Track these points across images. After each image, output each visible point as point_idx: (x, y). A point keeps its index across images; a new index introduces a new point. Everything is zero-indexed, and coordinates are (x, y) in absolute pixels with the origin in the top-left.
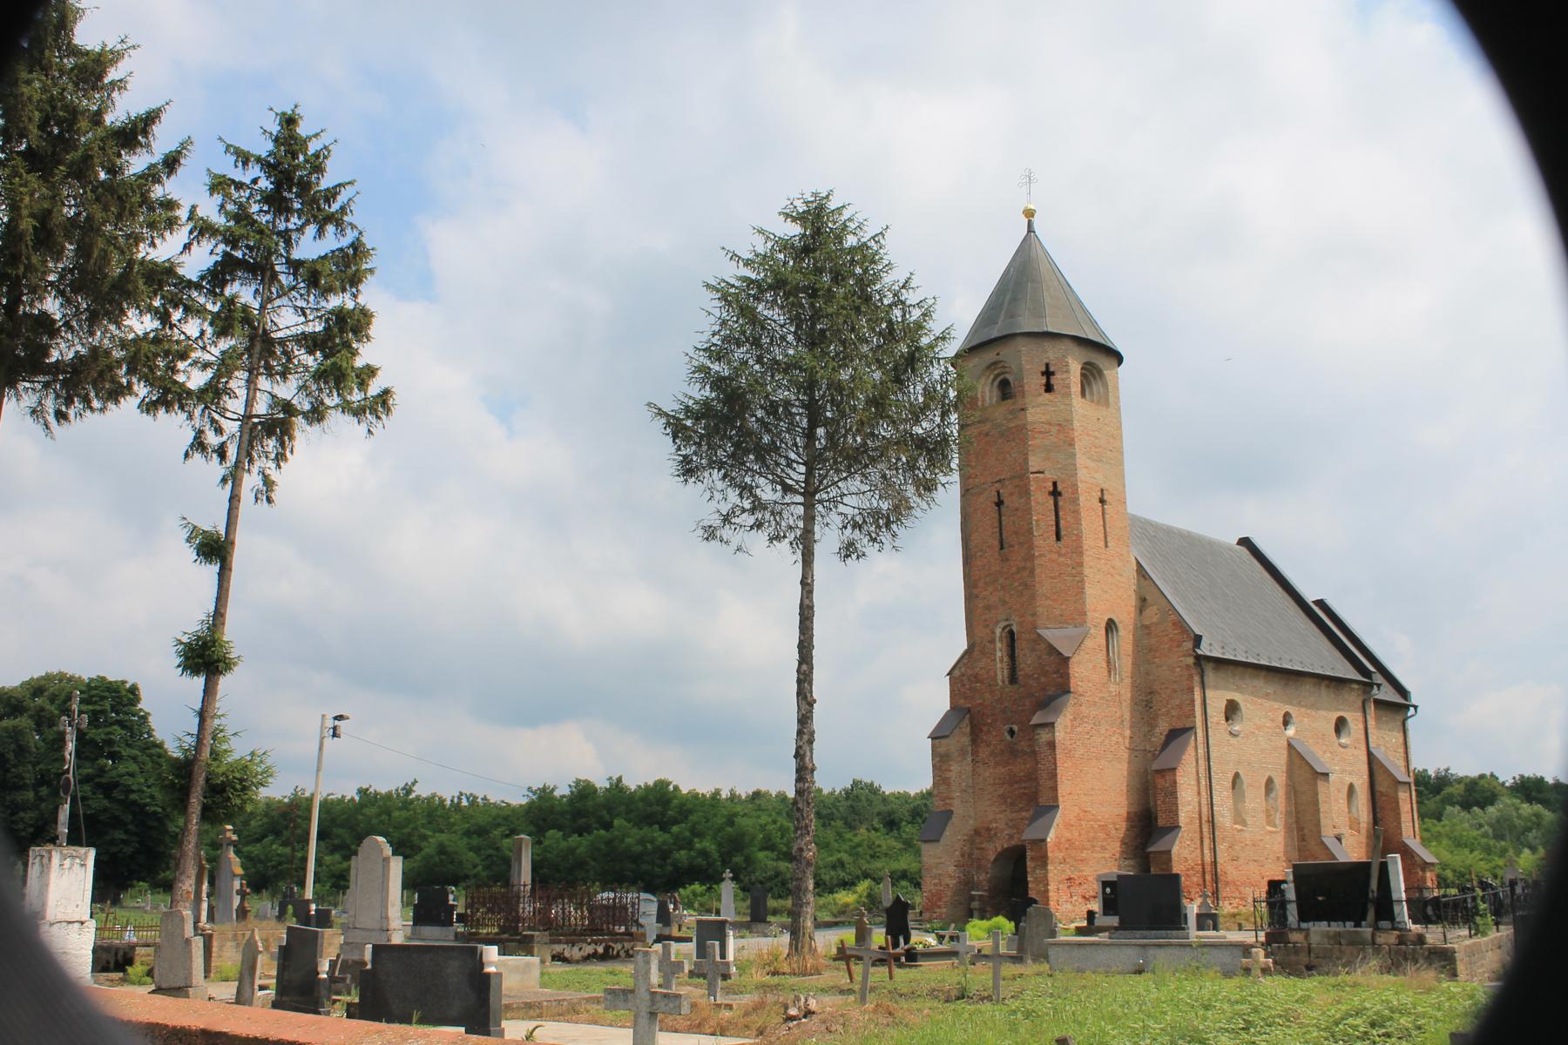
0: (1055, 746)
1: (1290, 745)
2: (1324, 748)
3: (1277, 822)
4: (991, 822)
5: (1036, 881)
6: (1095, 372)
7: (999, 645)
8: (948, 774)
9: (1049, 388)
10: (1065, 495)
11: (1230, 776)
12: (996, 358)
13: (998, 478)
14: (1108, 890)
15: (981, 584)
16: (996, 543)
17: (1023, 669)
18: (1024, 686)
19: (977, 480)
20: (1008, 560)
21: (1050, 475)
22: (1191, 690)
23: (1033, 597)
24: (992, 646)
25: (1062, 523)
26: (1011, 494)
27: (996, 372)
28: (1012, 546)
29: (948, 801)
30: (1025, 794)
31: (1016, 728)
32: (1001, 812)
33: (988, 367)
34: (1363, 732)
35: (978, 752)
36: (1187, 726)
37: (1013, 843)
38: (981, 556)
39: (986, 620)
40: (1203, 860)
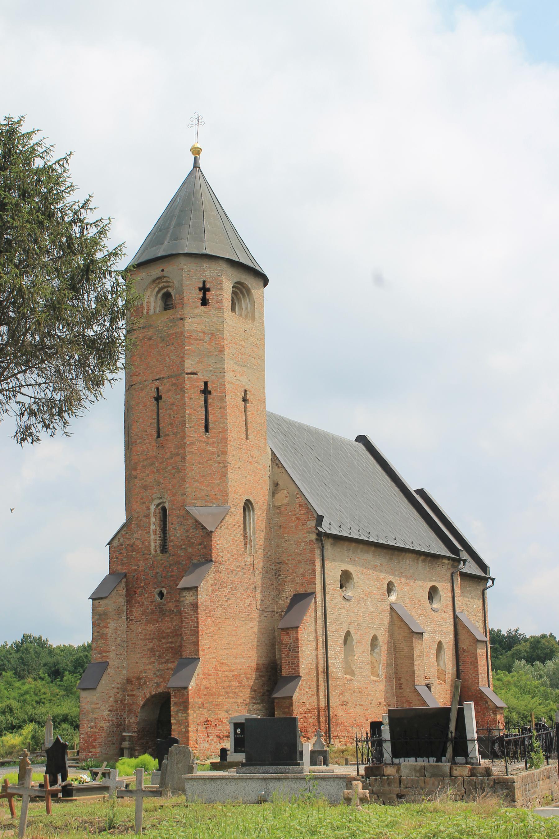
0: (197, 607)
1: (392, 608)
2: (419, 612)
3: (380, 673)
4: (141, 672)
5: (179, 723)
6: (244, 290)
7: (153, 519)
8: (105, 631)
9: (204, 302)
10: (214, 394)
11: (343, 634)
13: (157, 377)
14: (239, 731)
15: (139, 467)
16: (154, 432)
17: (172, 541)
19: (140, 378)
20: (164, 447)
21: (202, 376)
22: (313, 562)
23: (183, 479)
24: (147, 520)
25: (211, 417)
26: (169, 391)
27: (160, 286)
28: (168, 435)
29: (104, 654)
30: (171, 648)
31: (165, 591)
32: (150, 663)
33: (154, 281)
34: (451, 599)
35: (131, 611)
36: (308, 592)
37: (160, 690)
38: (140, 443)
39: (142, 498)
40: (318, 705)
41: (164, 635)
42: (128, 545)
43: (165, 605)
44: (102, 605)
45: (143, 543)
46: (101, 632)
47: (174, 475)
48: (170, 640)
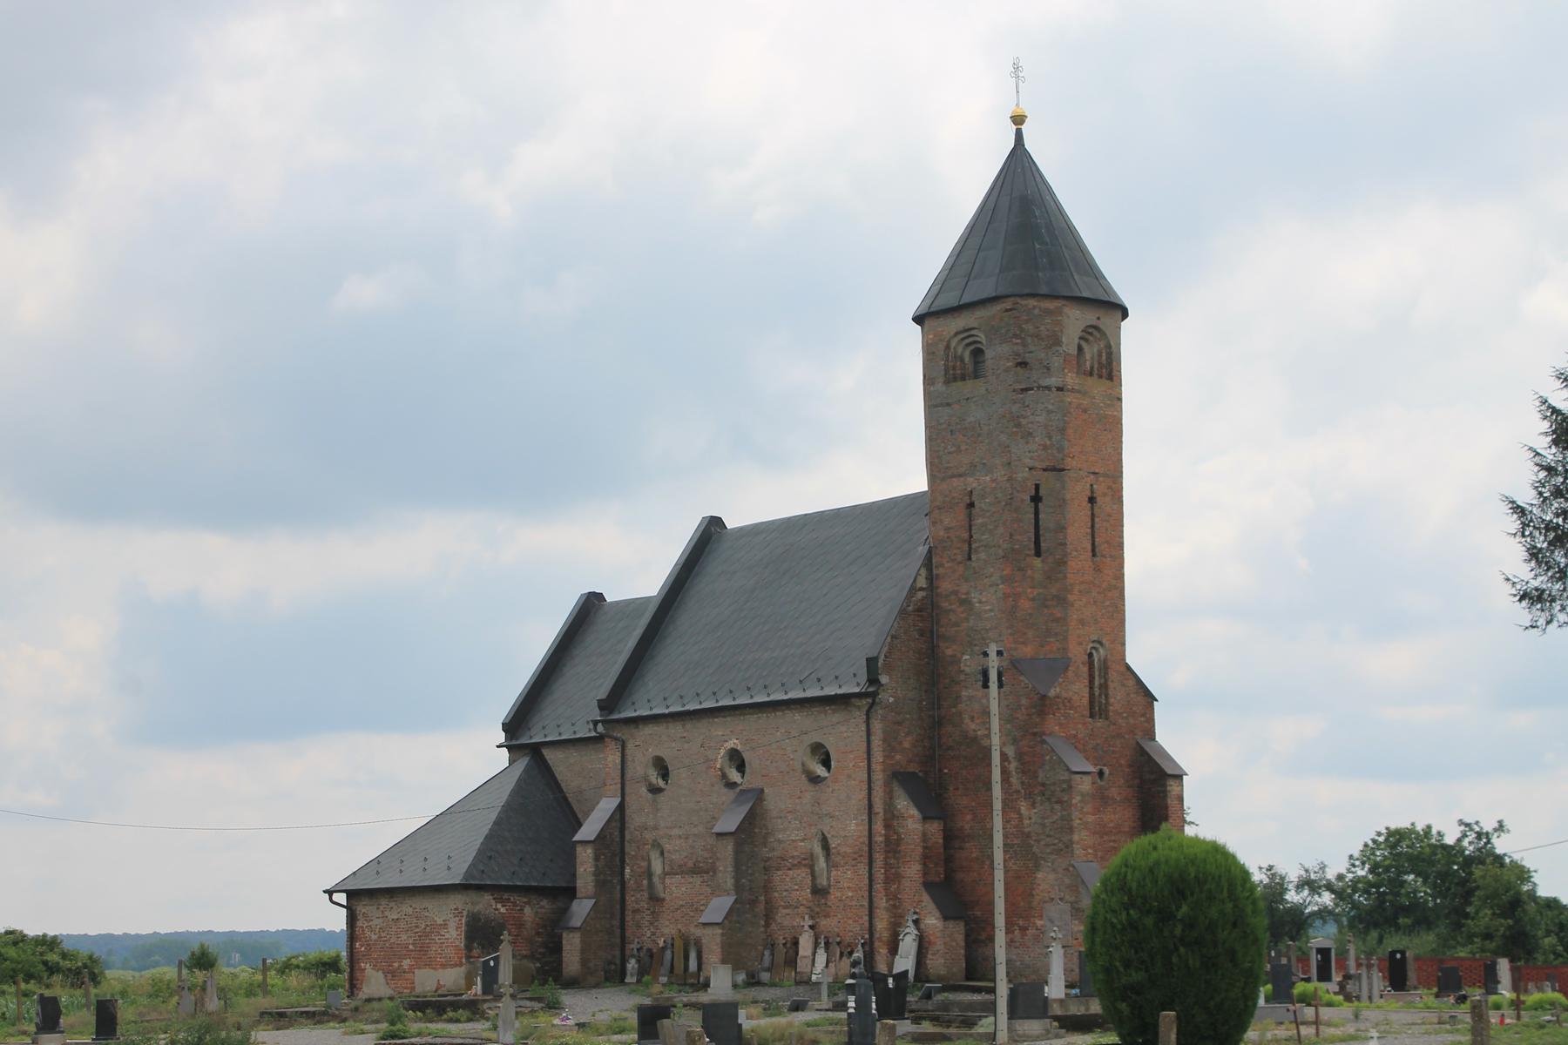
12: (1094, 322)
18: (1114, 724)
19: (1074, 462)
26: (1105, 495)
28: (1103, 556)
31: (1106, 770)
39: (1079, 637)
46: (1084, 819)
47: (1113, 615)
48: (1113, 838)
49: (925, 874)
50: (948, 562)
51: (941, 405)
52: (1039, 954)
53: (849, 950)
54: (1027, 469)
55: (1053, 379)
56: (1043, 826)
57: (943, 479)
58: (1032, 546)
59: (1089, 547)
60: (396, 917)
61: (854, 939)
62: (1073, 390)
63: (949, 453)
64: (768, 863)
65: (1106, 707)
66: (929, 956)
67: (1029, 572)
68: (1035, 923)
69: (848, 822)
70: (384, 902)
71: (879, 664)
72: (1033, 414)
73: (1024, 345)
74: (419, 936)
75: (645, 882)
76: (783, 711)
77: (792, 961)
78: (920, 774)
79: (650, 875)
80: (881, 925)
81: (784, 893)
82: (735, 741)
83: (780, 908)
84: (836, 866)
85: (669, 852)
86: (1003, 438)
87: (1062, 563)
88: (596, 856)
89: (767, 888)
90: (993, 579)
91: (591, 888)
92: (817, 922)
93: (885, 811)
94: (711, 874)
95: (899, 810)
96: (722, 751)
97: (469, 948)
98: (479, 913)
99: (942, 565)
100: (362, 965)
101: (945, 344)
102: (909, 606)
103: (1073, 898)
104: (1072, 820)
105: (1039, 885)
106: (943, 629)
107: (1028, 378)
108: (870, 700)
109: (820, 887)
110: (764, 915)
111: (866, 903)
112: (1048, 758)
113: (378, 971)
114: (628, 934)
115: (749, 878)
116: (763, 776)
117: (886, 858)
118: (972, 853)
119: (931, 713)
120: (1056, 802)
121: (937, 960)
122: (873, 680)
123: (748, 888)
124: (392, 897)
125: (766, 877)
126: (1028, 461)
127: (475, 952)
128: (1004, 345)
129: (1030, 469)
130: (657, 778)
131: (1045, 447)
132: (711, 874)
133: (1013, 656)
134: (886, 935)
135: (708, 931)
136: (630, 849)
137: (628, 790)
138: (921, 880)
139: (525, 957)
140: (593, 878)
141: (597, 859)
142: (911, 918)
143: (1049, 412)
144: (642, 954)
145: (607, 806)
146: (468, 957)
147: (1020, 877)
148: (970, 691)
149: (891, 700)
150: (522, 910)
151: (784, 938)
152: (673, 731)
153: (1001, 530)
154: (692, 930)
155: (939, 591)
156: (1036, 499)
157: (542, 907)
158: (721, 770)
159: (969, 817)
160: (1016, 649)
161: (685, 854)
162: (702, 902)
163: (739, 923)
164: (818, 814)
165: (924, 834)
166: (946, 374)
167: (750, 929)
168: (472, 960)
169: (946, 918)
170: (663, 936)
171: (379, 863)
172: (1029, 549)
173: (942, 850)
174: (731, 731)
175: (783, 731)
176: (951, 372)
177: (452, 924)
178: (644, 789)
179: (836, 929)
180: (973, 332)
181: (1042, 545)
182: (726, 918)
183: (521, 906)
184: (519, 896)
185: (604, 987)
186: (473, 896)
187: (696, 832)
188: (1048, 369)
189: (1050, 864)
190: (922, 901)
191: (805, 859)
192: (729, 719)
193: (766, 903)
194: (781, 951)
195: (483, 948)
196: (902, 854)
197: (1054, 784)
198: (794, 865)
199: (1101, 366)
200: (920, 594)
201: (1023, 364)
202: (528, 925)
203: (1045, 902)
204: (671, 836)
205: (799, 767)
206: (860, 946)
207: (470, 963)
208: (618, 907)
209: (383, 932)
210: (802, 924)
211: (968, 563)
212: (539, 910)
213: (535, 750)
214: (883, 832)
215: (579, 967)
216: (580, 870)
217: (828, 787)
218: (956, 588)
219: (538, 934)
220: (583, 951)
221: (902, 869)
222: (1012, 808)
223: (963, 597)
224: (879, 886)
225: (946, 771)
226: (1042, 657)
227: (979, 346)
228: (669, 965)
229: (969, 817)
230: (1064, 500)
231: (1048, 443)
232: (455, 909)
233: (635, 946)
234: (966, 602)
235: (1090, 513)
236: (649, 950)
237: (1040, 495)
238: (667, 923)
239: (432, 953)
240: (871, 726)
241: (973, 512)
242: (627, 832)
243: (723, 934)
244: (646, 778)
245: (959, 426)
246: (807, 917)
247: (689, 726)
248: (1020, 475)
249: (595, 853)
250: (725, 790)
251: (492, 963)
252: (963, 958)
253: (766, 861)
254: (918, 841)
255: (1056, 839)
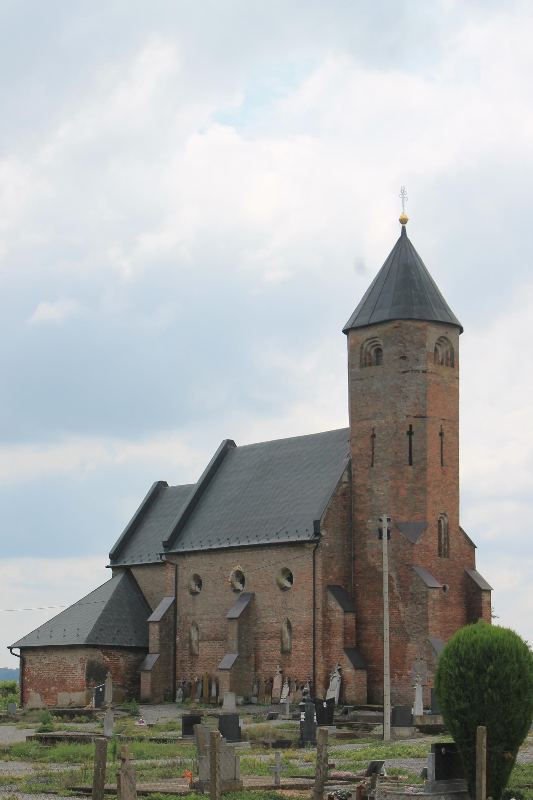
12: (444, 335)
13: (442, 417)
18: (452, 561)
19: (432, 413)
26: (448, 432)
28: (447, 466)
30: (451, 630)
31: (448, 587)
41: (447, 620)
42: (425, 545)
43: (448, 597)
44: (435, 593)
45: (434, 546)
46: (435, 613)
47: (452, 499)
48: (451, 625)
49: (345, 643)
50: (360, 468)
51: (358, 380)
52: (409, 690)
53: (302, 685)
54: (406, 416)
55: (421, 366)
56: (412, 617)
57: (358, 421)
58: (408, 459)
59: (440, 461)
60: (47, 663)
61: (305, 679)
62: (431, 373)
63: (362, 406)
64: (257, 636)
65: (448, 551)
66: (347, 690)
67: (406, 474)
68: (407, 672)
69: (302, 613)
70: (41, 654)
71: (321, 524)
72: (409, 386)
73: (405, 347)
74: (60, 674)
75: (188, 645)
76: (266, 549)
77: (269, 691)
78: (343, 587)
79: (190, 641)
80: (320, 671)
81: (266, 653)
82: (240, 566)
83: (263, 661)
84: (295, 638)
85: (201, 628)
86: (392, 398)
87: (424, 469)
88: (160, 630)
89: (256, 650)
90: (385, 477)
91: (157, 648)
92: (284, 669)
93: (323, 607)
94: (225, 641)
95: (331, 607)
96: (232, 572)
97: (88, 681)
98: (94, 661)
99: (357, 470)
100: (28, 689)
101: (360, 345)
102: (338, 492)
103: (428, 658)
104: (428, 614)
105: (409, 651)
106: (357, 506)
107: (407, 365)
108: (315, 545)
109: (286, 649)
110: (255, 665)
111: (311, 659)
112: (415, 579)
113: (37, 693)
114: (178, 673)
115: (246, 644)
116: (255, 586)
117: (323, 634)
118: (371, 631)
119: (349, 552)
120: (419, 604)
121: (351, 692)
122: (317, 533)
123: (245, 649)
124: (45, 651)
125: (255, 643)
126: (406, 412)
127: (92, 683)
128: (393, 347)
129: (407, 416)
130: (195, 586)
131: (416, 404)
132: (225, 641)
133: (396, 521)
134: (322, 677)
135: (222, 673)
136: (179, 626)
137: (179, 593)
138: (343, 646)
139: (119, 686)
140: (159, 642)
141: (161, 631)
142: (337, 668)
143: (418, 385)
144: (185, 686)
145: (167, 602)
146: (88, 686)
147: (398, 646)
148: (372, 540)
149: (327, 544)
150: (119, 660)
151: (265, 678)
152: (205, 560)
153: (390, 450)
154: (214, 672)
155: (355, 484)
156: (410, 433)
157: (130, 658)
158: (231, 582)
159: (370, 612)
160: (398, 517)
161: (210, 630)
162: (219, 657)
163: (240, 669)
164: (285, 608)
165: (345, 621)
166: (360, 363)
167: (246, 673)
168: (90, 687)
169: (356, 668)
170: (197, 675)
171: (39, 631)
172: (406, 462)
173: (355, 630)
174: (237, 561)
175: (266, 561)
176: (364, 361)
177: (79, 667)
178: (188, 593)
179: (294, 674)
180: (376, 339)
181: (413, 459)
182: (233, 666)
183: (119, 658)
184: (116, 652)
185: (163, 704)
186: (91, 651)
187: (217, 617)
188: (418, 360)
189: (415, 639)
190: (343, 659)
191: (277, 634)
192: (236, 554)
193: (256, 658)
194: (263, 685)
195: (96, 680)
196: (333, 632)
197: (418, 594)
198: (271, 637)
199: (447, 359)
200: (344, 486)
201: (404, 358)
202: (122, 668)
203: (412, 660)
204: (202, 619)
205: (275, 582)
206: (308, 683)
207: (89, 689)
208: (172, 659)
209: (40, 671)
210: (275, 670)
211: (372, 468)
212: (128, 660)
213: (127, 570)
214: (322, 619)
215: (150, 693)
216: (151, 638)
217: (291, 593)
218: (364, 482)
219: (127, 673)
220: (152, 683)
221: (332, 640)
222: (394, 607)
223: (369, 487)
224: (319, 650)
225: (357, 585)
226: (412, 522)
227: (379, 347)
228: (200, 692)
229: (370, 612)
230: (426, 434)
231: (417, 402)
232: (81, 659)
233: (181, 681)
234: (370, 490)
235: (440, 441)
236: (190, 683)
237: (413, 431)
238: (200, 668)
239: (67, 683)
240: (316, 559)
241: (375, 440)
242: (178, 617)
243: (231, 675)
244: (189, 586)
245: (368, 392)
246: (278, 666)
247: (214, 557)
248: (401, 419)
249: (160, 628)
250: (233, 594)
251: (101, 690)
252: (366, 691)
253: (255, 634)
254: (341, 624)
255: (419, 625)
